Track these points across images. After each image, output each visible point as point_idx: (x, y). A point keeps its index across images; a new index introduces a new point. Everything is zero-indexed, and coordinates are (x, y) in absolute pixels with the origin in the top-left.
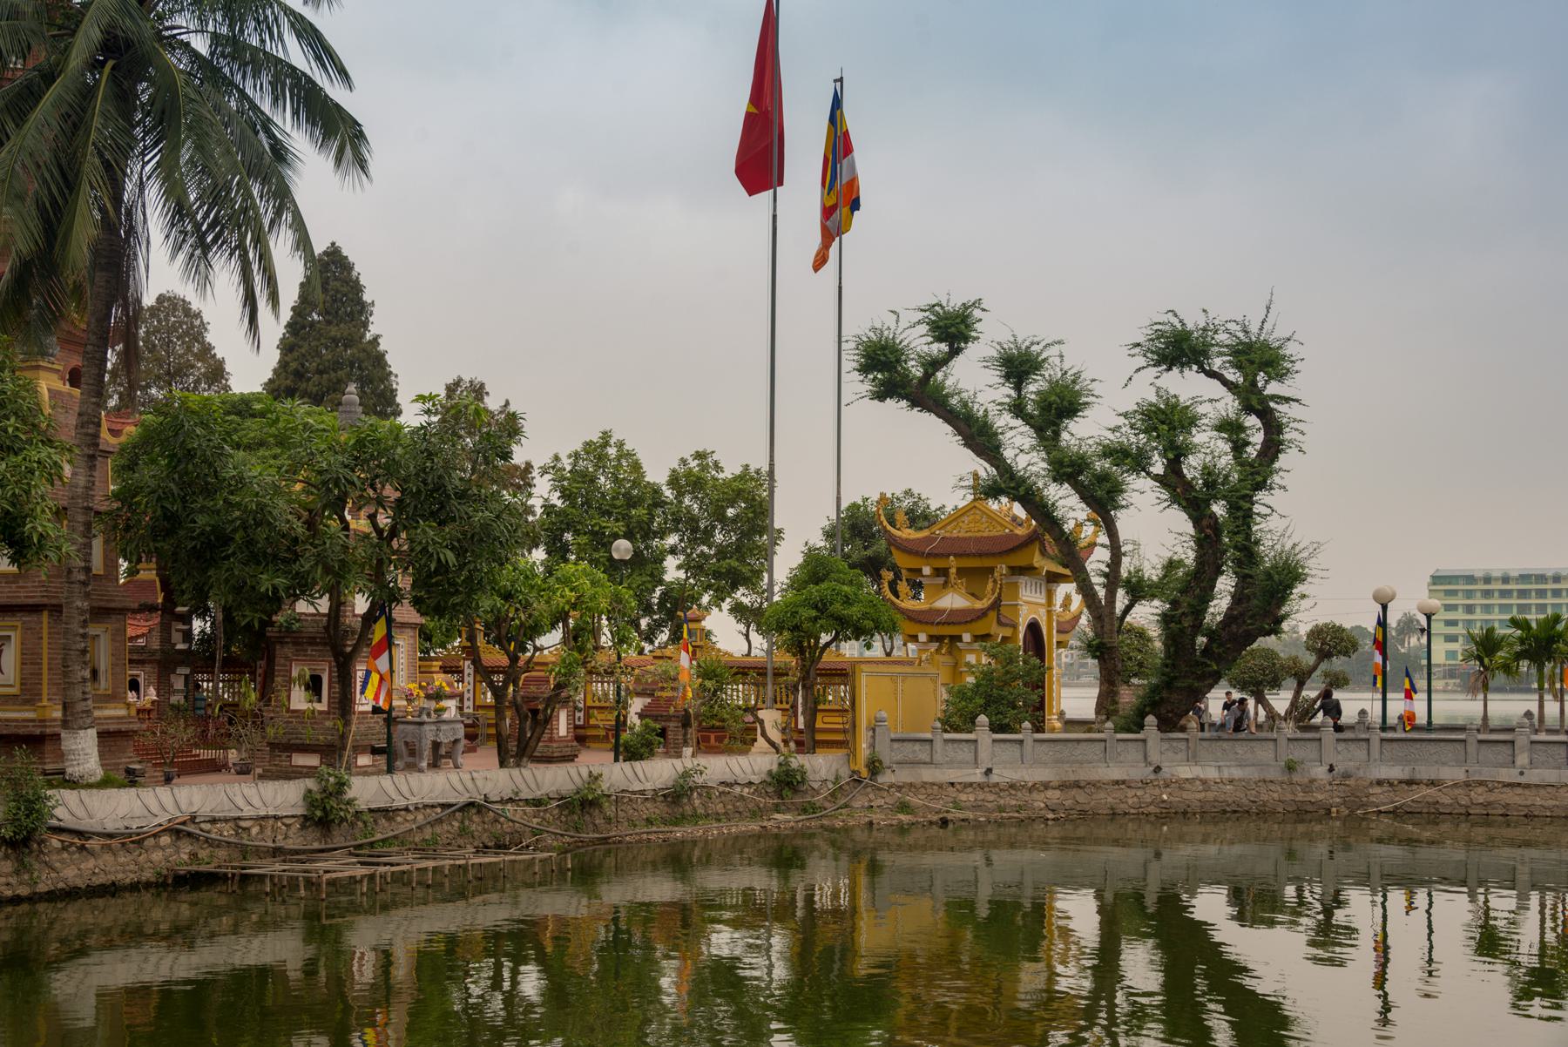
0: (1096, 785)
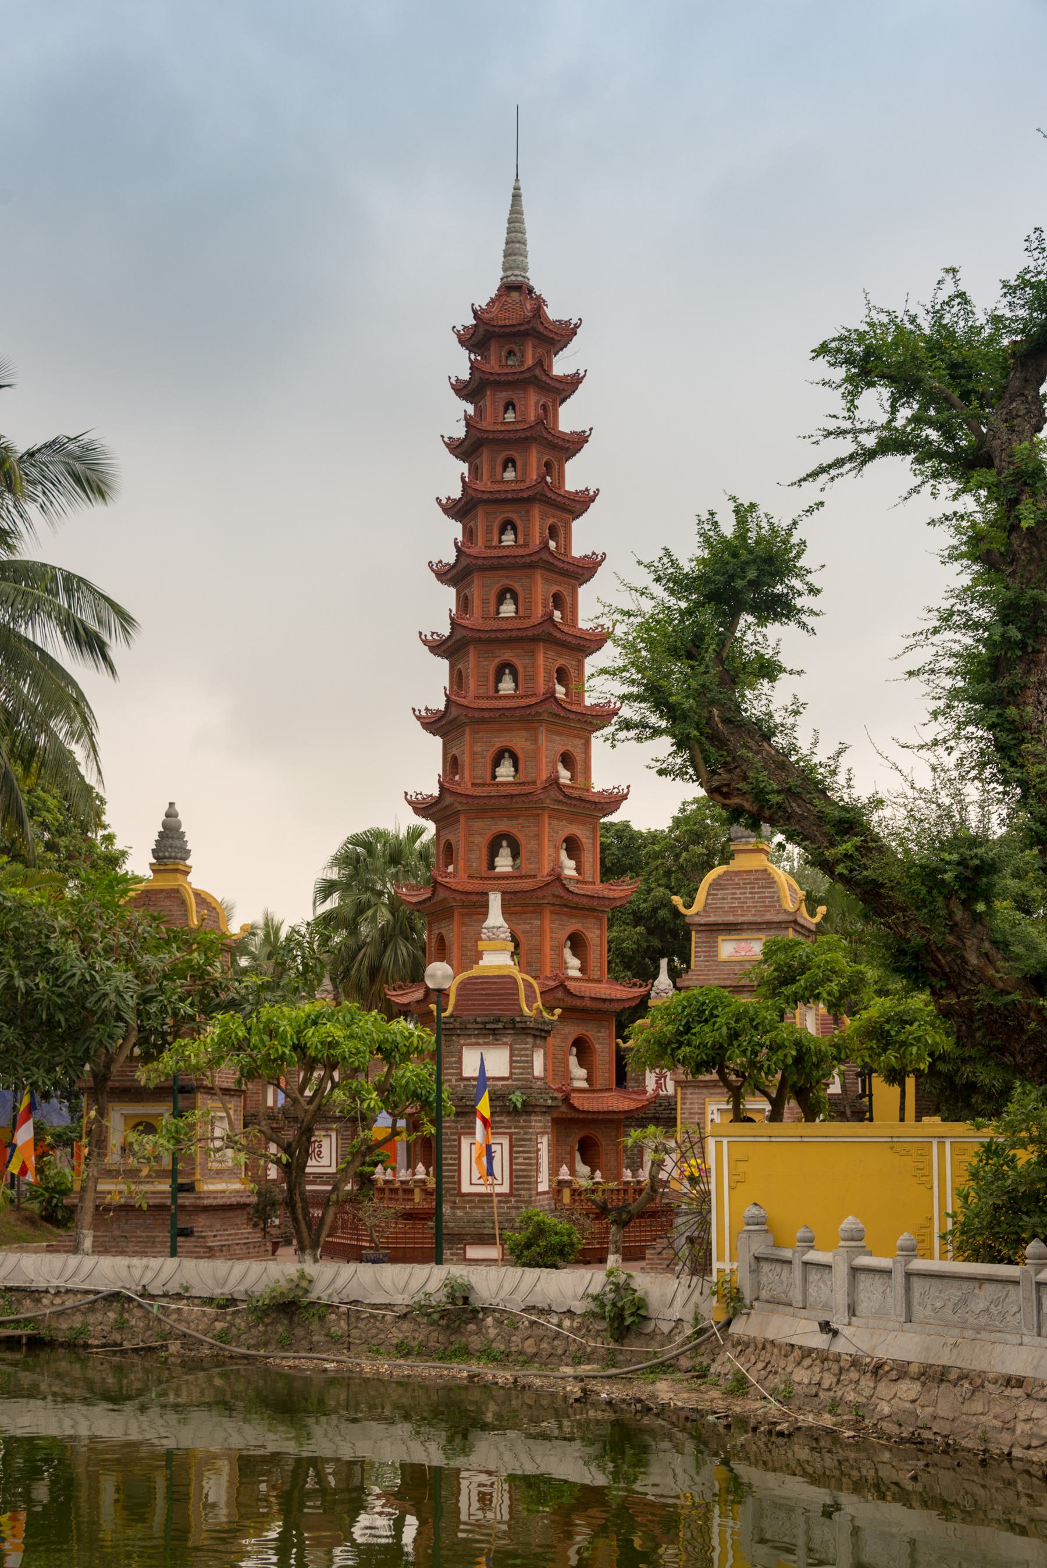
0: (973, 1382)
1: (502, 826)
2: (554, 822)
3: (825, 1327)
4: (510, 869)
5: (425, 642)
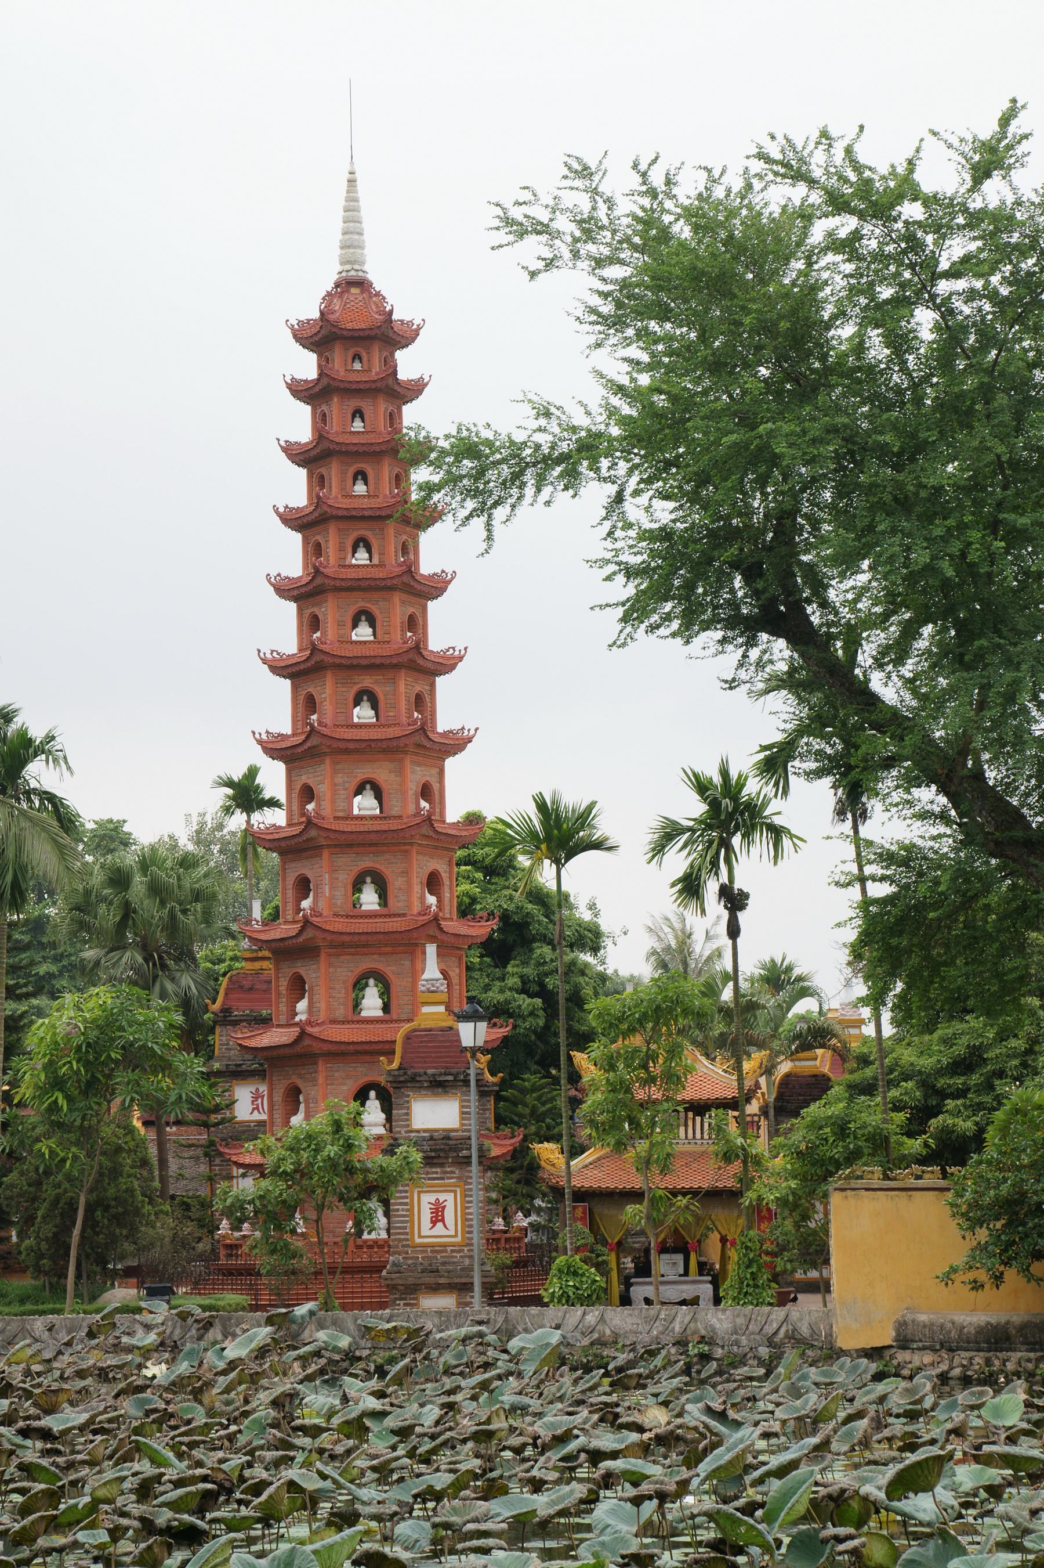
2: (420, 857)
4: (377, 907)
5: (264, 661)
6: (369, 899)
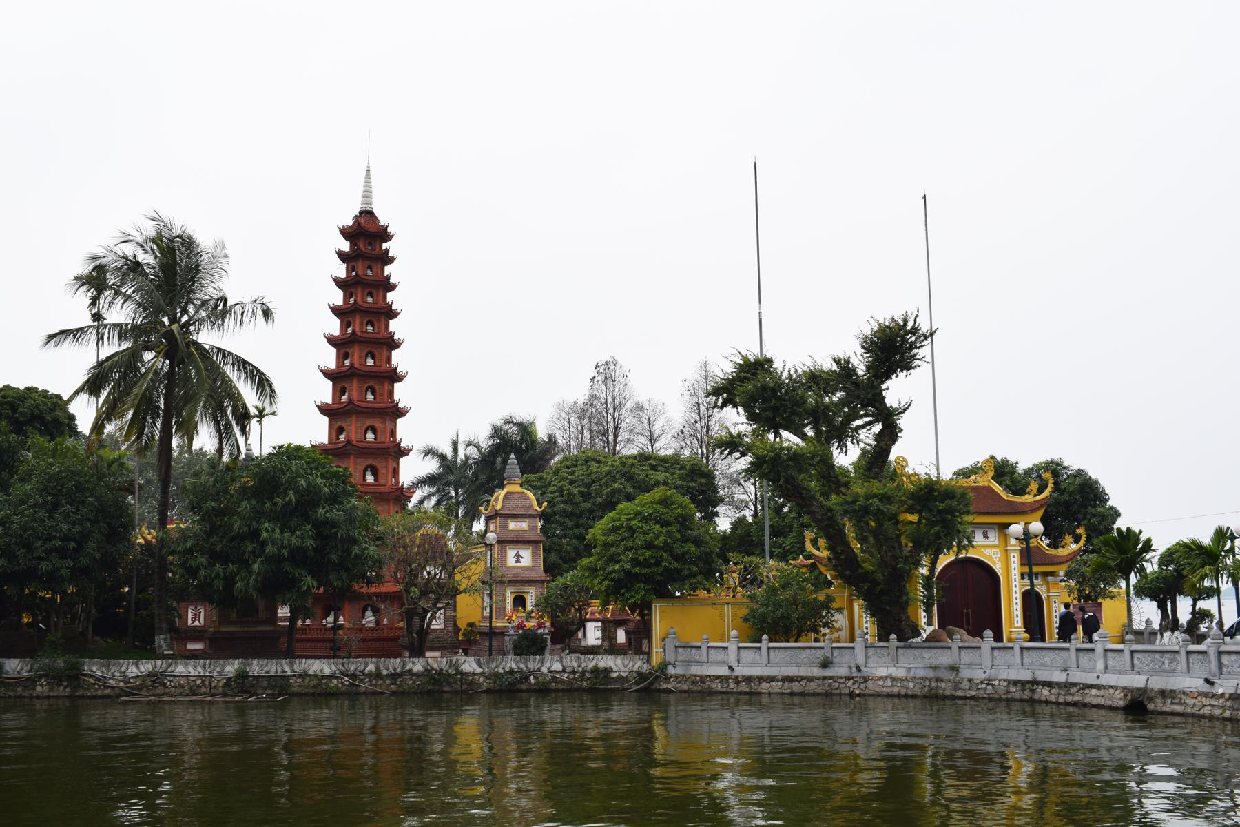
1: (370, 462)
3: (731, 668)
6: (370, 478)
